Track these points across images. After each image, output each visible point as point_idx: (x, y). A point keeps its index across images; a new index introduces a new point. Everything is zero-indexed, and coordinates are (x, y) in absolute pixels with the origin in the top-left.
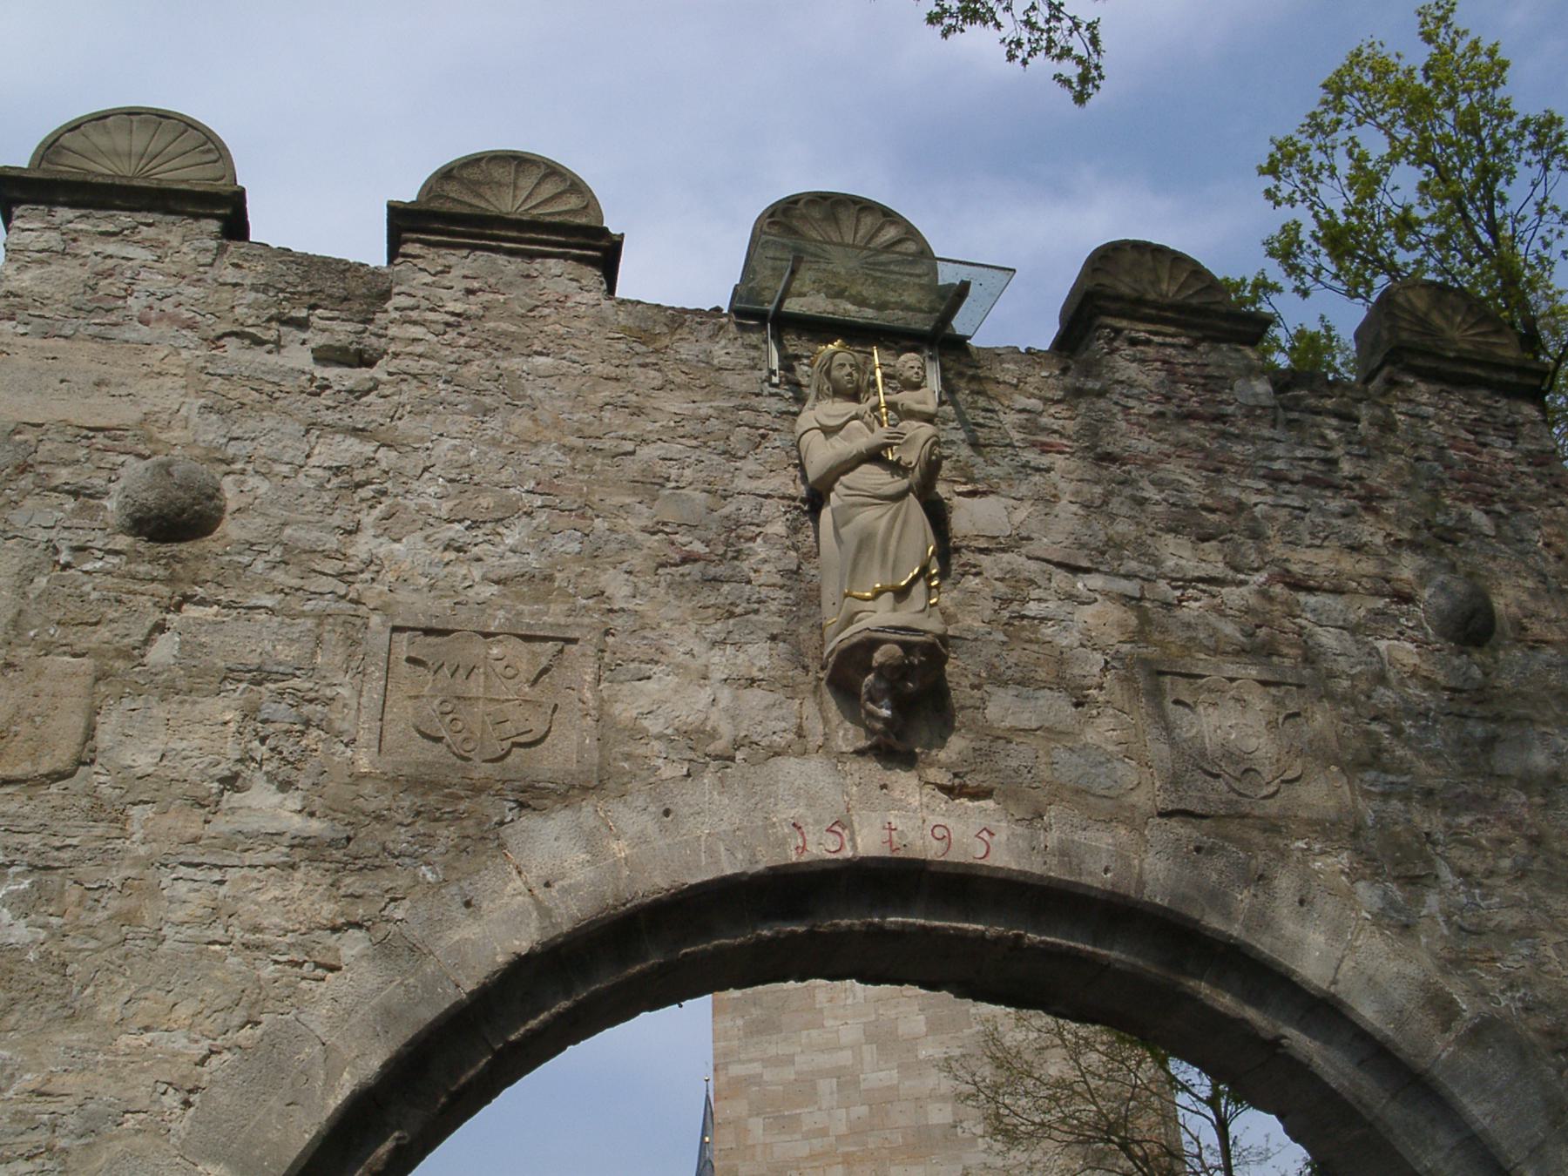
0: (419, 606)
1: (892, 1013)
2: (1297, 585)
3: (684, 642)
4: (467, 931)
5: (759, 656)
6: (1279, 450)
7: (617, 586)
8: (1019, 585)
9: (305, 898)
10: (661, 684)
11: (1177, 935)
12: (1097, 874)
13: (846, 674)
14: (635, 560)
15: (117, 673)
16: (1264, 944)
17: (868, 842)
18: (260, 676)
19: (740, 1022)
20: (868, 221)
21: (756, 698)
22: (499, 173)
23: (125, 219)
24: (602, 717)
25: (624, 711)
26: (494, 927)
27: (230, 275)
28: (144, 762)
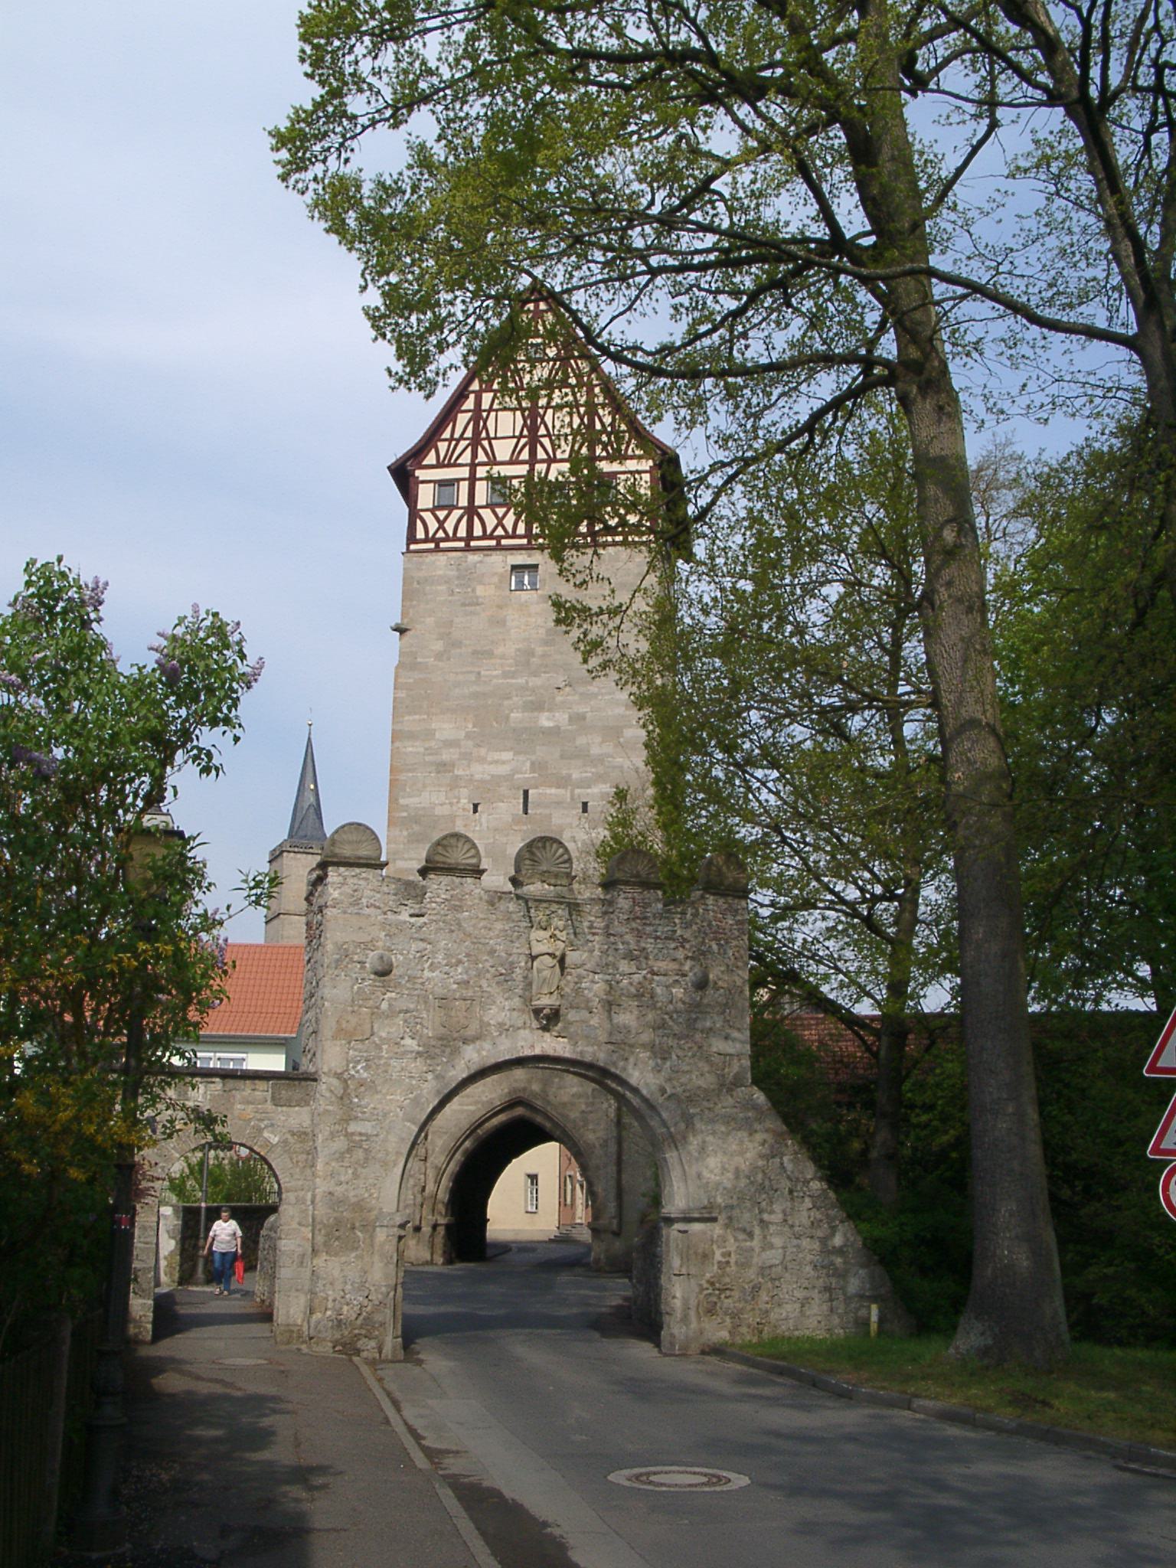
0: (440, 991)
1: (504, 840)
2: (654, 973)
3: (499, 1000)
4: (452, 1073)
5: (517, 1002)
6: (660, 928)
7: (484, 983)
8: (580, 977)
9: (420, 1065)
10: (494, 1010)
11: (605, 1072)
12: (588, 1059)
13: (537, 1012)
14: (488, 976)
15: (375, 1013)
16: (624, 1076)
17: (537, 1051)
18: (406, 1012)
19: (405, 833)
20: (555, 846)
21: (515, 1014)
22: (453, 841)
23: (358, 870)
24: (481, 1021)
25: (486, 1019)
26: (460, 1072)
27: (385, 889)
28: (384, 1035)
